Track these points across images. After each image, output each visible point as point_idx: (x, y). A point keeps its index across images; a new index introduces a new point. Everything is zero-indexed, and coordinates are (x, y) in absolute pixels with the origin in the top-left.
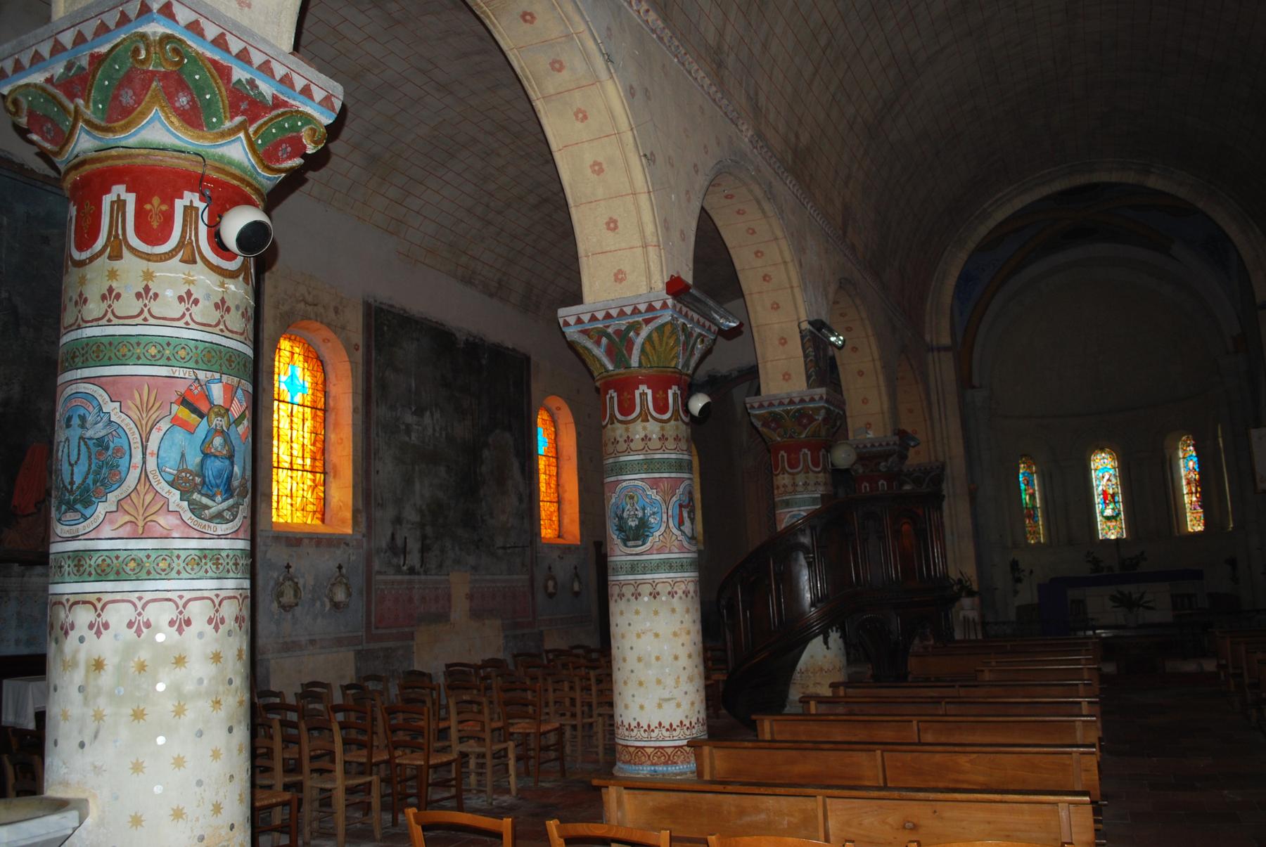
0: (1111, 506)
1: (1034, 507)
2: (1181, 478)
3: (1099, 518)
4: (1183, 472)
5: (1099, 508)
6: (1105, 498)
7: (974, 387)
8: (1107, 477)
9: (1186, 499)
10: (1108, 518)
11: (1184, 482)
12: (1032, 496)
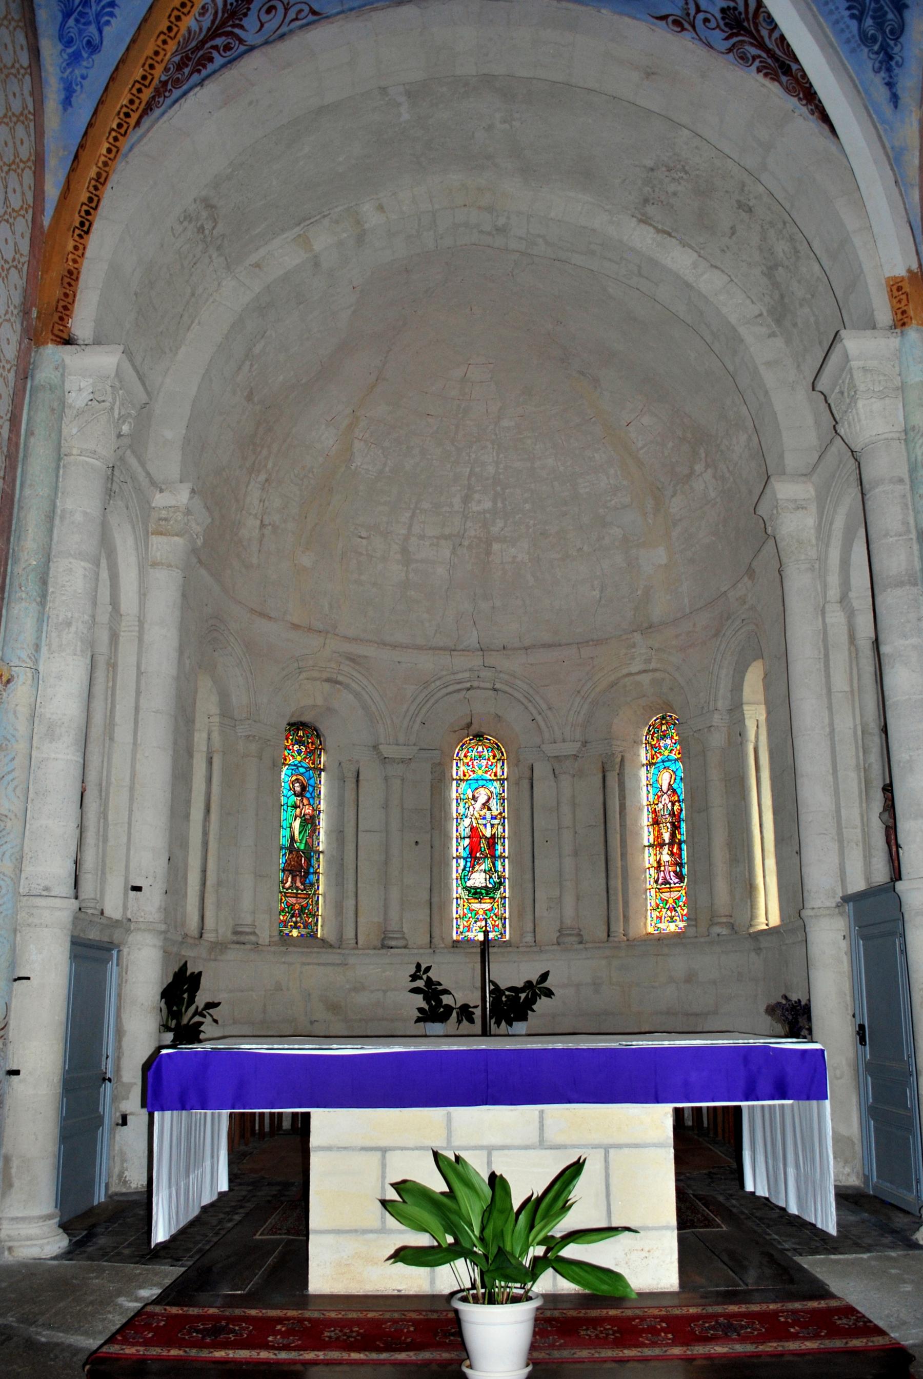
0: (486, 865)
1: (310, 852)
2: (640, 809)
3: (456, 890)
4: (645, 796)
5: (456, 868)
6: (473, 849)
7: (68, 341)
8: (482, 799)
9: (649, 858)
10: (476, 893)
11: (645, 819)
12: (310, 822)
